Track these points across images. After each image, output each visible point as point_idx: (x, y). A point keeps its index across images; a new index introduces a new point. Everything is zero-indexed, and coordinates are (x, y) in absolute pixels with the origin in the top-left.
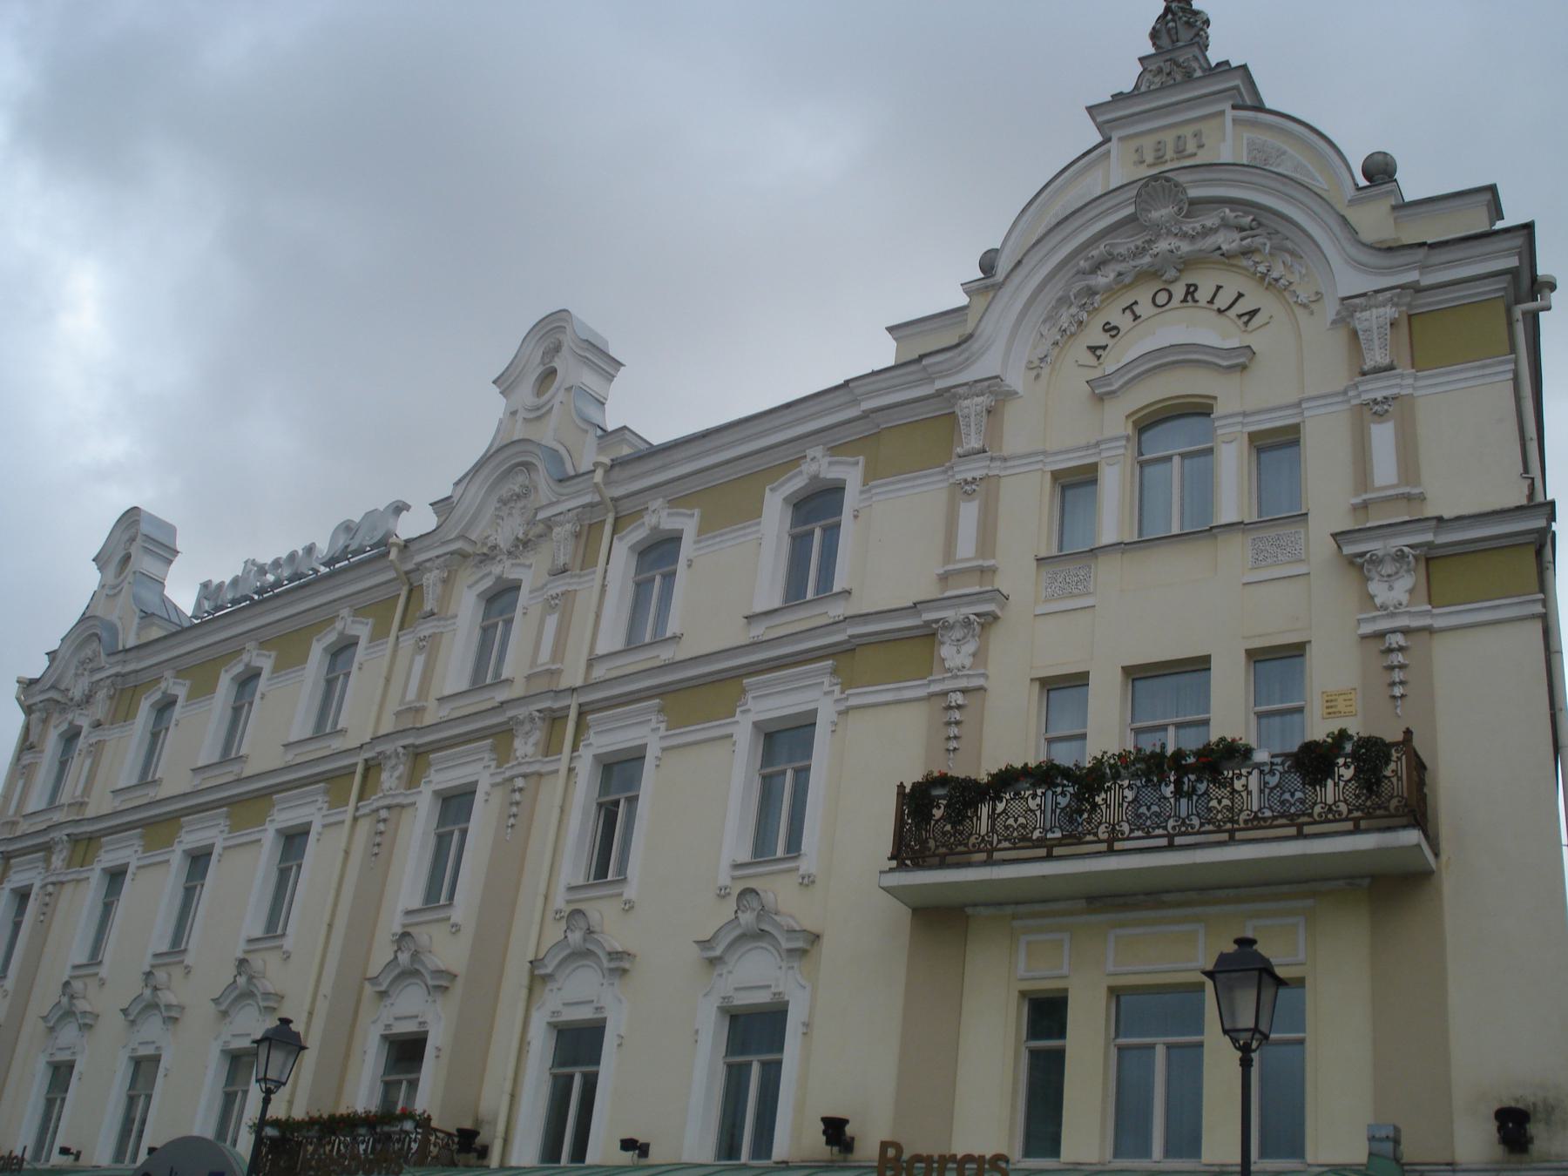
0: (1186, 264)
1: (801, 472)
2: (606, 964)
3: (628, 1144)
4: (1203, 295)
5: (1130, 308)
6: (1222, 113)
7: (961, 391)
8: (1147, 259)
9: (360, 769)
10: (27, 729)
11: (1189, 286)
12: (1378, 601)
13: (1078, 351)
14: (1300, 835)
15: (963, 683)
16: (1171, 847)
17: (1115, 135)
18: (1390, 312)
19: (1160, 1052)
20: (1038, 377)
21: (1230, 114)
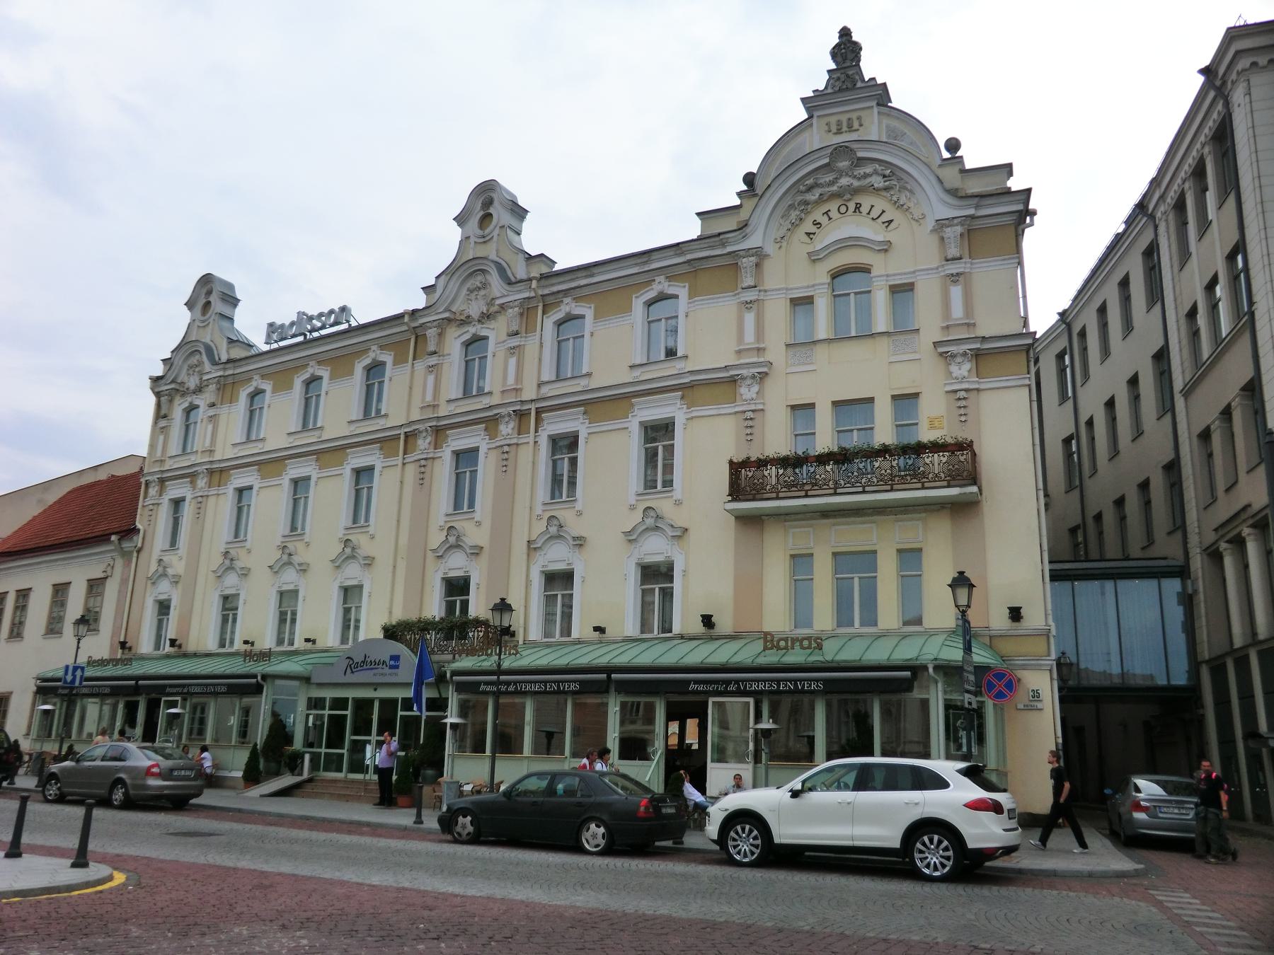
0: (856, 191)
1: (652, 289)
2: (571, 542)
3: (597, 629)
4: (864, 209)
5: (826, 213)
6: (872, 107)
7: (741, 253)
8: (835, 188)
9: (402, 437)
10: (159, 405)
11: (857, 204)
12: (954, 375)
13: (800, 233)
14: (923, 488)
15: (753, 407)
16: (864, 492)
17: (816, 114)
18: (959, 229)
19: (856, 581)
20: (780, 247)
21: (876, 110)
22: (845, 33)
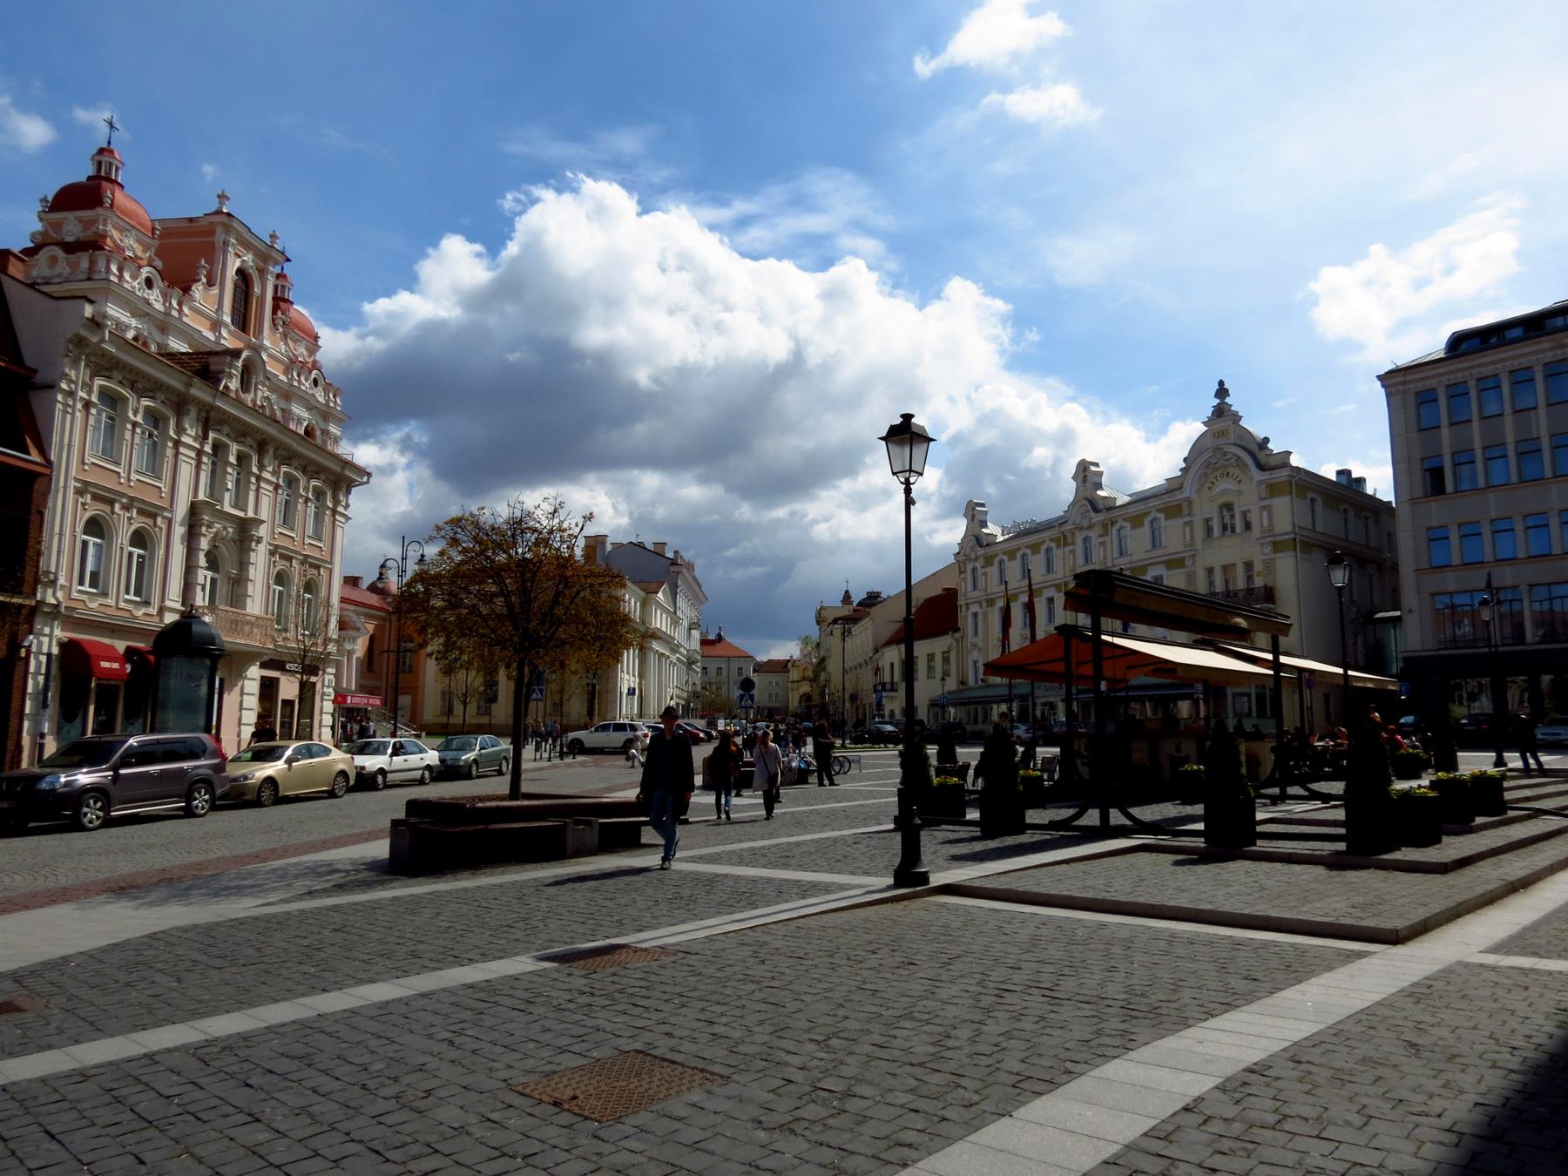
13: (1206, 488)
22: (1221, 383)
